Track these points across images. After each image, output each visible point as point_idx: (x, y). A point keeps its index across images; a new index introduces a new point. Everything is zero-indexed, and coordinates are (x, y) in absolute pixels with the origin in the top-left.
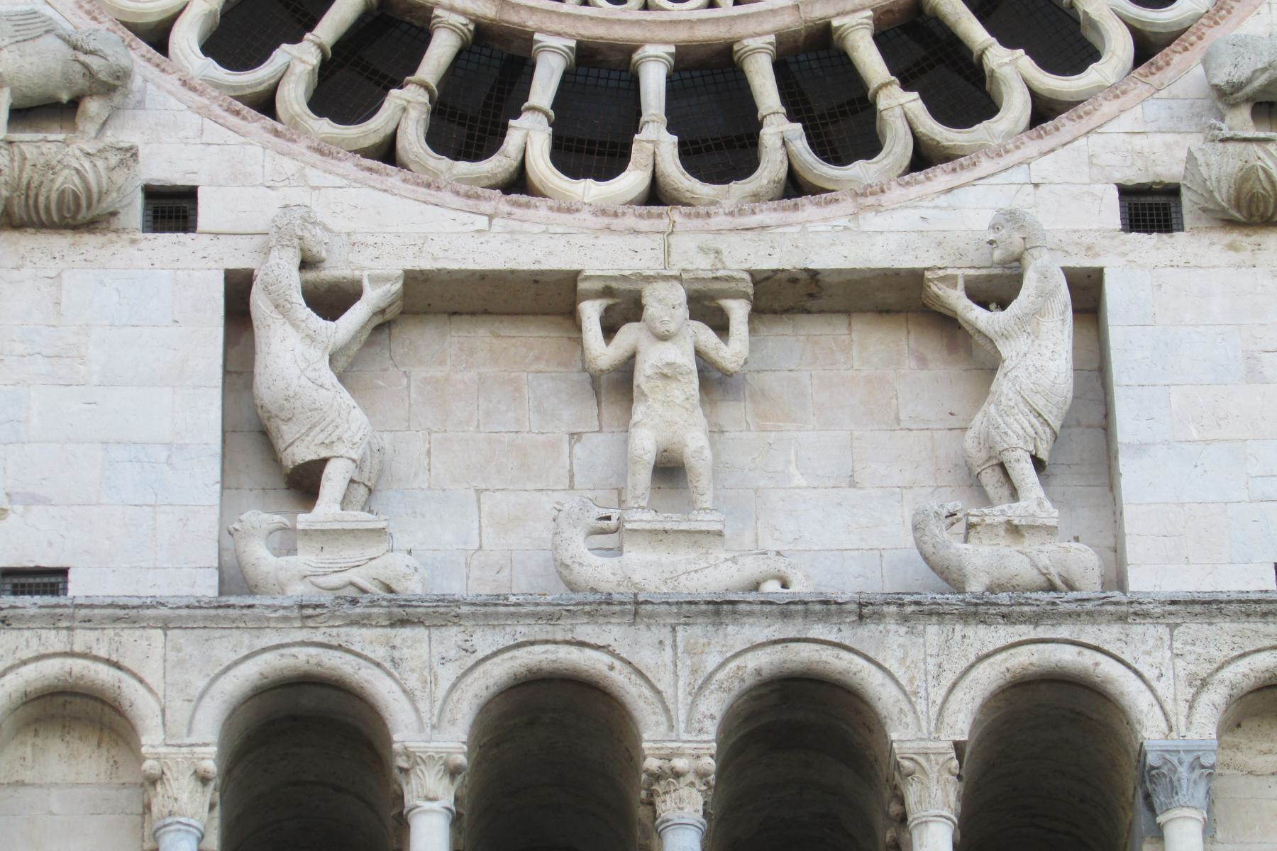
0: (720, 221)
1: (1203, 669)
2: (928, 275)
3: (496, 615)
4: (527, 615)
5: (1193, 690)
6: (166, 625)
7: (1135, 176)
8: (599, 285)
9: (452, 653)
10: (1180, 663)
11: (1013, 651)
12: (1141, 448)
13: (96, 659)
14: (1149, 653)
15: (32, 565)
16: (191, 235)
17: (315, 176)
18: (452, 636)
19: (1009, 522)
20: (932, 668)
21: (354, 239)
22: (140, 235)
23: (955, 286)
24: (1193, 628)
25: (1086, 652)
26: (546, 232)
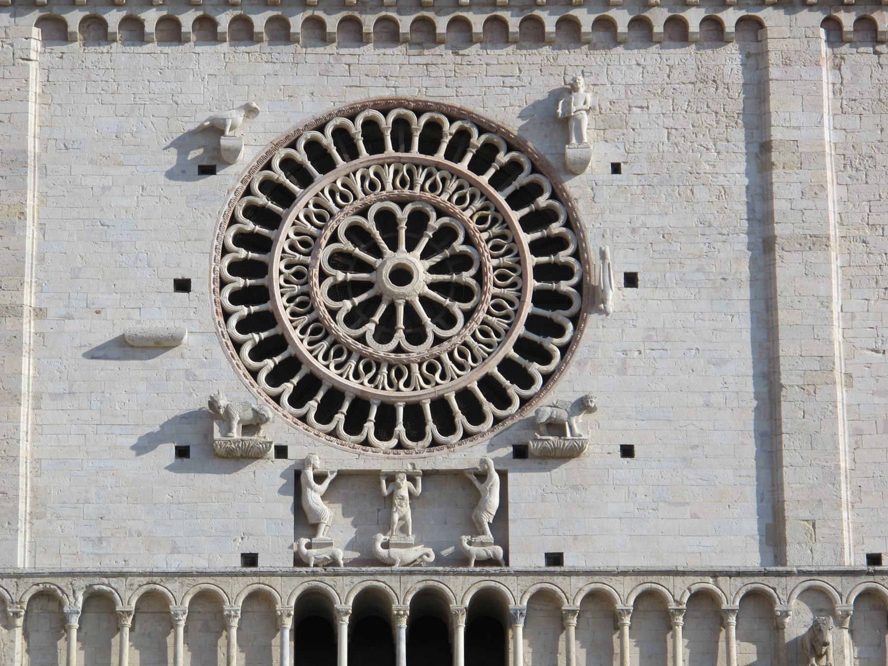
0: (414, 454)
2: (465, 471)
6: (282, 576)
7: (516, 442)
8: (384, 474)
13: (265, 585)
18: (349, 578)
21: (326, 461)
23: (471, 473)
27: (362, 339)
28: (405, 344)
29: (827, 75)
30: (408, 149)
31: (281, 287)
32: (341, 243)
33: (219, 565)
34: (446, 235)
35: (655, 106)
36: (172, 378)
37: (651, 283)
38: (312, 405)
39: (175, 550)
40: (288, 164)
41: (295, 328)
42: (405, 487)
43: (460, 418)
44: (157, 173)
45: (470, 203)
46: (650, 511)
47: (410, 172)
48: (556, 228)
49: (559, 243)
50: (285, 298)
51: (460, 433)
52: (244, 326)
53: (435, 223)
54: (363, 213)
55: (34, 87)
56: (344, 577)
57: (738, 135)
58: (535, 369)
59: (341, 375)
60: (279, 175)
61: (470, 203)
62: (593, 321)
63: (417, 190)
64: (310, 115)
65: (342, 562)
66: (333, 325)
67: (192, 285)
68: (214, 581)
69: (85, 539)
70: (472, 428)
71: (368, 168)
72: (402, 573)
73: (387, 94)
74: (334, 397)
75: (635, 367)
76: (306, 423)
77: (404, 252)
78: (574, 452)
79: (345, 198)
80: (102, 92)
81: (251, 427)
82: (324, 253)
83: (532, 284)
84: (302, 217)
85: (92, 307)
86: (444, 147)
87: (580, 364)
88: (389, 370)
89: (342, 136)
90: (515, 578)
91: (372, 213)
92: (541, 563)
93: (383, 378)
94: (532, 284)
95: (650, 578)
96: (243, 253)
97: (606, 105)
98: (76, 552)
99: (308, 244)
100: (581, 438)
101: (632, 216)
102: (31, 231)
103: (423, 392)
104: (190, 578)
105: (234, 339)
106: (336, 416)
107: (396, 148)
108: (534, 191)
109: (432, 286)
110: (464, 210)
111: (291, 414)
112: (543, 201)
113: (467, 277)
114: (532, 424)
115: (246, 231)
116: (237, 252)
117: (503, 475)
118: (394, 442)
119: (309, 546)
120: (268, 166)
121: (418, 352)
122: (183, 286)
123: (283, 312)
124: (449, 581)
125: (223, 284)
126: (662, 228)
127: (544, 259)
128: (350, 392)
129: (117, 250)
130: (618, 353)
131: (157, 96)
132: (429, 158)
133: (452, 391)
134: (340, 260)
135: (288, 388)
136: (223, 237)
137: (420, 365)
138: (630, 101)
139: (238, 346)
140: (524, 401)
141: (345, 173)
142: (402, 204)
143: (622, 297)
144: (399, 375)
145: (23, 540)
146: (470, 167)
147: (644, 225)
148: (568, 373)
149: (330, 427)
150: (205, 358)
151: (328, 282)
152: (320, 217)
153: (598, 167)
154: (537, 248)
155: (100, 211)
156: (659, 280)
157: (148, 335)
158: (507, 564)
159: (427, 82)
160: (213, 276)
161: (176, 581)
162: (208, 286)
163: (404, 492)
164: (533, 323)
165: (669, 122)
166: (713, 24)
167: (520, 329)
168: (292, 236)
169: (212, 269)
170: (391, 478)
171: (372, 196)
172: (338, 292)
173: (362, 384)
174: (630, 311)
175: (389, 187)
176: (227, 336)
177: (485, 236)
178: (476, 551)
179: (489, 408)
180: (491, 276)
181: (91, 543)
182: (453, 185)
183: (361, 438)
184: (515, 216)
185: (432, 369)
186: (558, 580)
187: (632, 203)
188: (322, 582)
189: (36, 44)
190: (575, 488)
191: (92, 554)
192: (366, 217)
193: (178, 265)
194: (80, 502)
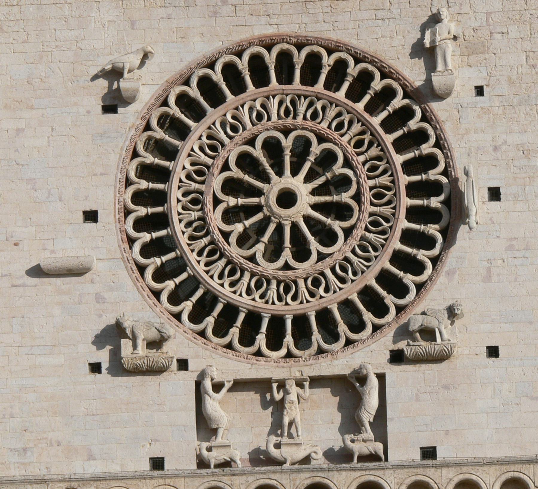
0: (302, 362)
1: (401, 481)
3: (253, 473)
4: (259, 473)
5: (398, 486)
6: (185, 477)
9: (244, 482)
10: (396, 479)
11: (360, 478)
12: (392, 419)
13: (171, 486)
14: (389, 477)
15: (156, 457)
16: (187, 372)
17: (214, 355)
18: (244, 477)
19: (363, 439)
20: (343, 482)
22: (176, 372)
23: (353, 378)
24: (399, 471)
25: (376, 477)
26: (264, 368)
27: (252, 259)
28: (292, 262)
30: (289, 80)
31: (179, 214)
32: (232, 171)
33: (131, 468)
35: (514, 31)
36: (83, 302)
37: (513, 196)
38: (210, 321)
39: (91, 457)
41: (192, 251)
42: (294, 390)
43: (343, 328)
44: (65, 114)
45: (348, 129)
46: (514, 406)
47: (293, 102)
50: (183, 224)
51: (343, 340)
54: (251, 142)
56: (240, 477)
59: (235, 292)
61: (348, 129)
63: (300, 118)
64: (201, 54)
65: (239, 462)
66: (226, 247)
67: (99, 215)
68: (125, 484)
69: (11, 450)
70: (353, 336)
71: (254, 100)
72: (292, 471)
73: (270, 31)
75: (499, 275)
76: (205, 338)
77: (289, 177)
79: (234, 129)
80: (14, 42)
84: (196, 149)
85: (11, 239)
86: (323, 78)
87: (448, 274)
88: (278, 286)
90: (392, 472)
91: (259, 143)
92: (417, 456)
93: (272, 293)
95: (513, 468)
96: (144, 184)
97: (469, 33)
98: (3, 461)
100: (449, 342)
101: (494, 135)
103: (308, 305)
104: (104, 482)
105: (138, 263)
106: (231, 330)
107: (280, 82)
109: (315, 207)
110: (342, 135)
111: (191, 330)
115: (146, 163)
116: (139, 184)
117: (381, 377)
118: (283, 352)
119: (209, 449)
120: (165, 103)
123: (181, 237)
124: (333, 477)
125: (127, 212)
126: (522, 144)
127: (416, 178)
128: (243, 307)
129: (32, 187)
130: (484, 262)
131: (62, 43)
132: (309, 88)
133: (334, 303)
135: (187, 306)
136: (126, 170)
137: (306, 280)
138: (492, 27)
139: (142, 269)
140: (400, 309)
141: (234, 106)
142: (286, 132)
143: (486, 210)
144: (287, 289)
146: (348, 95)
147: (505, 143)
148: (438, 282)
149: (226, 340)
150: (113, 282)
151: (221, 207)
152: (213, 148)
155: (15, 151)
156: (520, 194)
157: (61, 264)
158: (386, 459)
159: (305, 19)
160: (117, 206)
161: (91, 486)
162: (113, 216)
163: (293, 397)
165: (527, 46)
168: (188, 166)
169: (117, 200)
170: (282, 385)
171: (259, 126)
173: (254, 300)
174: (493, 223)
175: (274, 117)
176: (132, 262)
177: (362, 158)
180: (367, 196)
181: (17, 453)
182: (332, 112)
183: (253, 349)
185: (316, 283)
186: (431, 472)
187: (494, 123)
188: (221, 482)
190: (446, 387)
191: (18, 463)
192: (253, 146)
193: (86, 198)
194: (6, 417)
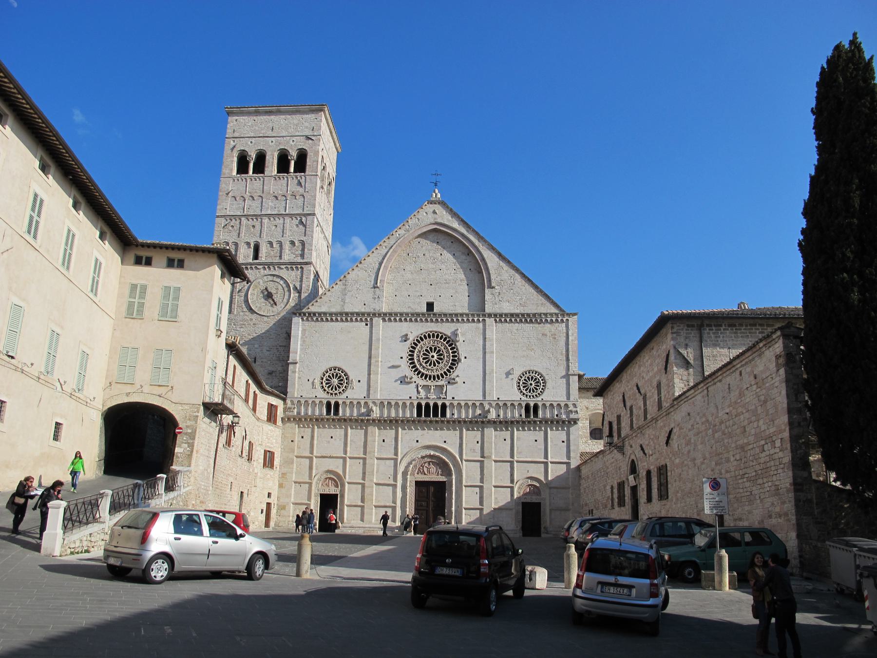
29: (494, 328)
34: (439, 351)
40: (417, 340)
42: (432, 387)
48: (455, 350)
49: (455, 352)
52: (410, 364)
53: (438, 349)
55: (381, 329)
57: (482, 336)
58: (452, 370)
60: (416, 342)
62: (460, 364)
74: (423, 374)
78: (457, 383)
81: (411, 379)
82: (422, 353)
83: (451, 358)
89: (425, 336)
94: (451, 358)
99: (420, 352)
102: (380, 350)
108: (452, 344)
112: (453, 346)
113: (442, 357)
114: (451, 378)
121: (434, 368)
122: (402, 358)
134: (424, 354)
135: (416, 373)
145: (379, 394)
153: (461, 341)
154: (452, 353)
164: (451, 364)
166: (478, 320)
167: (449, 365)
172: (424, 359)
178: (442, 397)
179: (445, 376)
184: (449, 348)
189: (381, 322)
